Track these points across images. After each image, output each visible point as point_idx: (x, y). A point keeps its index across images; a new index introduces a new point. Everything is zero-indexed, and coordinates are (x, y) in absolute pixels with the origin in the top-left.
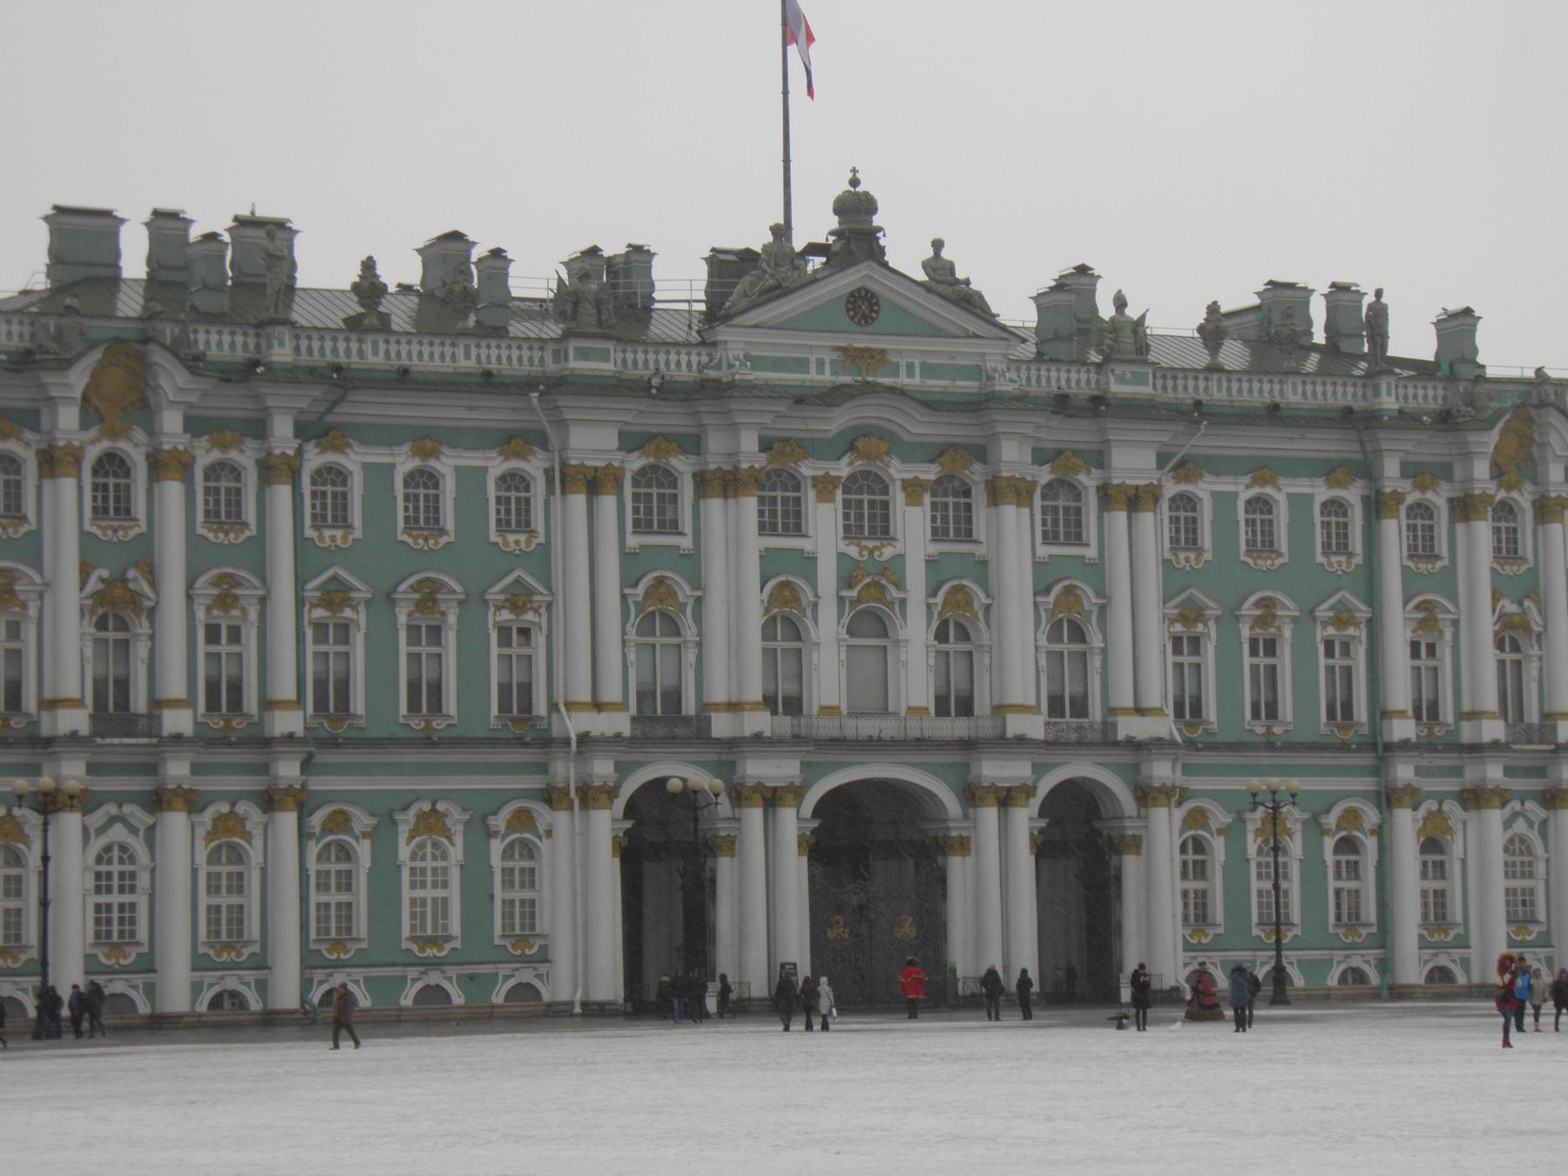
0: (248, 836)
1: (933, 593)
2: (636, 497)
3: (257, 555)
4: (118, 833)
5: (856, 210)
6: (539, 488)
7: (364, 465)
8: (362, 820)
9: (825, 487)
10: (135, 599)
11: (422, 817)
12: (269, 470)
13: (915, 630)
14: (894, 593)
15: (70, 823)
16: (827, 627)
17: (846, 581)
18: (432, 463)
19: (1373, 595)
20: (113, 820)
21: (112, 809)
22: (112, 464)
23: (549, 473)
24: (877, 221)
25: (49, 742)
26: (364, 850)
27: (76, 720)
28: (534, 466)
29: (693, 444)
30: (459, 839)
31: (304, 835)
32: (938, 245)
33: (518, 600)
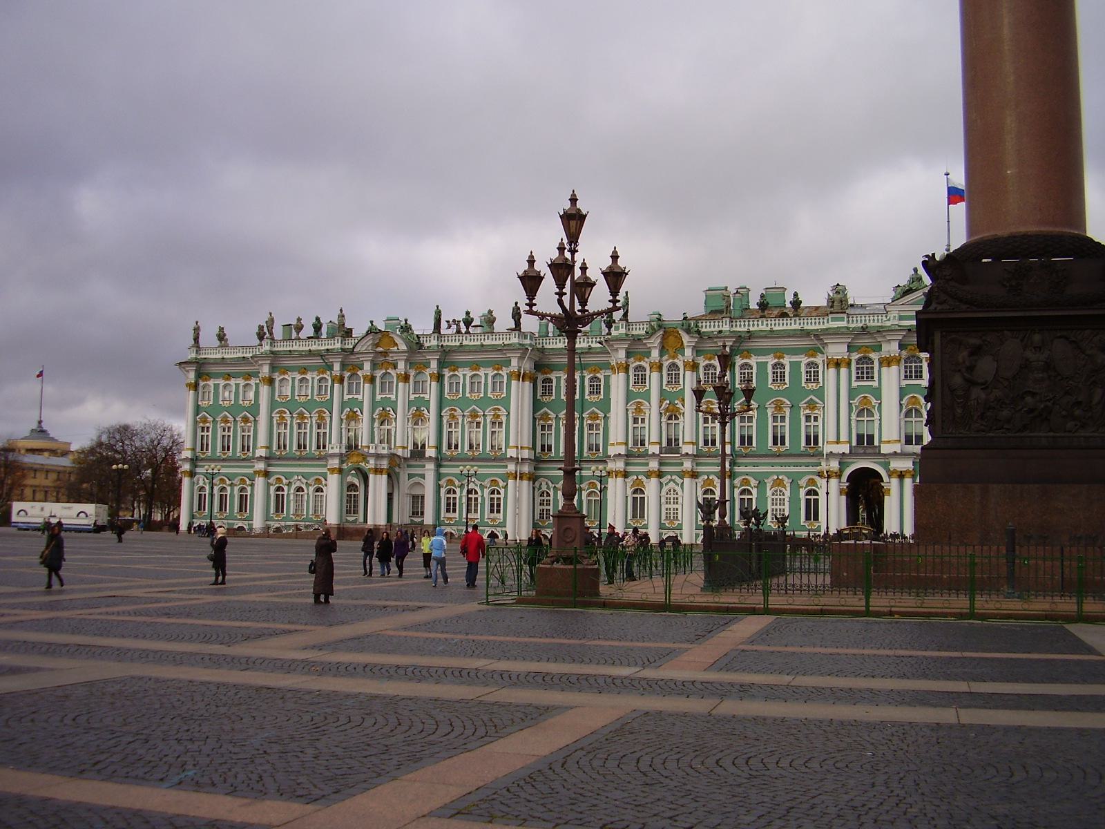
0: (715, 487)
2: (858, 368)
4: (672, 485)
7: (757, 363)
8: (753, 482)
11: (775, 481)
15: (654, 481)
18: (781, 360)
22: (674, 366)
23: (823, 361)
26: (754, 491)
28: (819, 359)
29: (878, 348)
30: (788, 489)
31: (733, 487)
33: (811, 405)
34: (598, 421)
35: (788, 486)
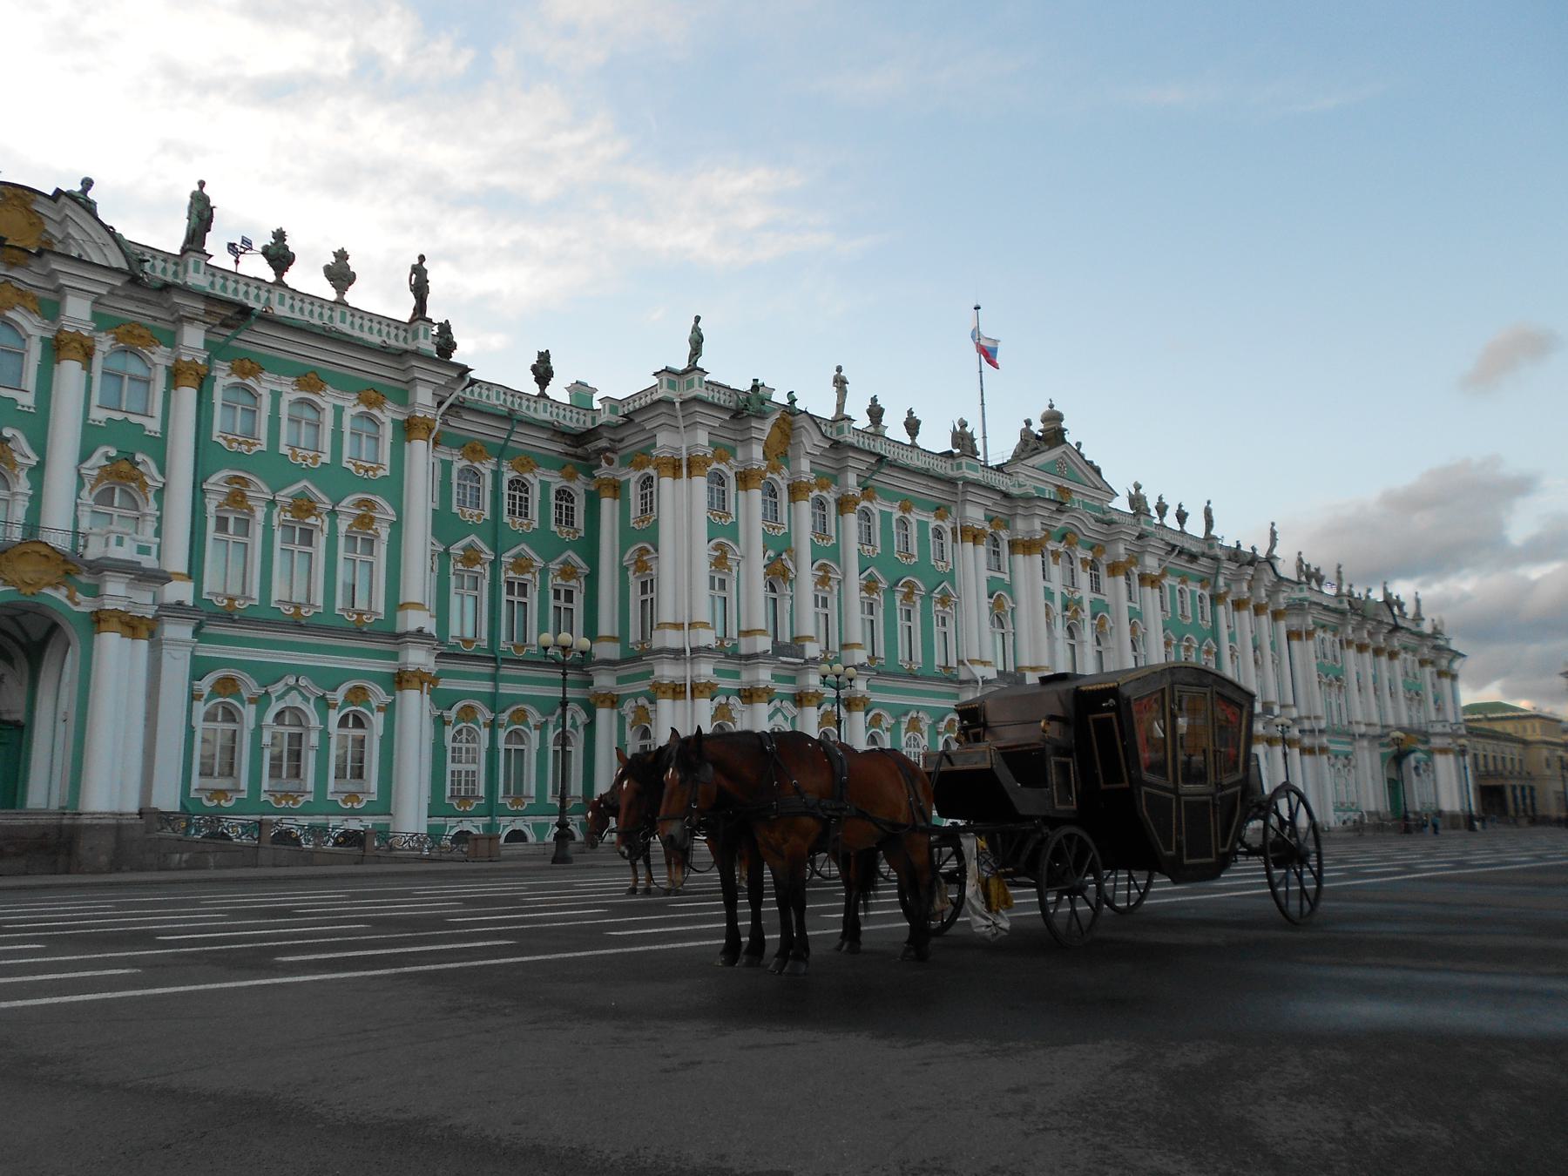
1: (1094, 617)
3: (835, 553)
5: (1053, 418)
6: (948, 537)
8: (888, 720)
9: (1056, 555)
10: (784, 573)
12: (844, 505)
13: (1087, 634)
14: (1082, 615)
16: (1060, 631)
17: (1066, 608)
19: (1216, 640)
20: (777, 710)
21: (777, 703)
24: (1064, 425)
25: (749, 657)
27: (764, 644)
28: (947, 526)
32: (1079, 444)
34: (528, 576)
35: (925, 728)
